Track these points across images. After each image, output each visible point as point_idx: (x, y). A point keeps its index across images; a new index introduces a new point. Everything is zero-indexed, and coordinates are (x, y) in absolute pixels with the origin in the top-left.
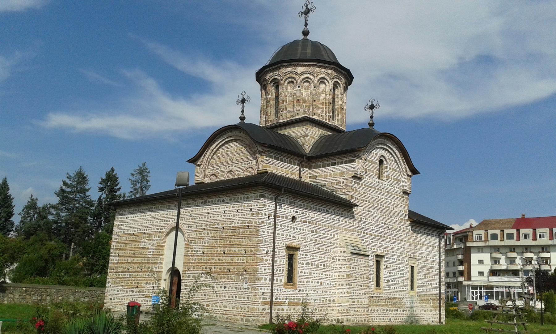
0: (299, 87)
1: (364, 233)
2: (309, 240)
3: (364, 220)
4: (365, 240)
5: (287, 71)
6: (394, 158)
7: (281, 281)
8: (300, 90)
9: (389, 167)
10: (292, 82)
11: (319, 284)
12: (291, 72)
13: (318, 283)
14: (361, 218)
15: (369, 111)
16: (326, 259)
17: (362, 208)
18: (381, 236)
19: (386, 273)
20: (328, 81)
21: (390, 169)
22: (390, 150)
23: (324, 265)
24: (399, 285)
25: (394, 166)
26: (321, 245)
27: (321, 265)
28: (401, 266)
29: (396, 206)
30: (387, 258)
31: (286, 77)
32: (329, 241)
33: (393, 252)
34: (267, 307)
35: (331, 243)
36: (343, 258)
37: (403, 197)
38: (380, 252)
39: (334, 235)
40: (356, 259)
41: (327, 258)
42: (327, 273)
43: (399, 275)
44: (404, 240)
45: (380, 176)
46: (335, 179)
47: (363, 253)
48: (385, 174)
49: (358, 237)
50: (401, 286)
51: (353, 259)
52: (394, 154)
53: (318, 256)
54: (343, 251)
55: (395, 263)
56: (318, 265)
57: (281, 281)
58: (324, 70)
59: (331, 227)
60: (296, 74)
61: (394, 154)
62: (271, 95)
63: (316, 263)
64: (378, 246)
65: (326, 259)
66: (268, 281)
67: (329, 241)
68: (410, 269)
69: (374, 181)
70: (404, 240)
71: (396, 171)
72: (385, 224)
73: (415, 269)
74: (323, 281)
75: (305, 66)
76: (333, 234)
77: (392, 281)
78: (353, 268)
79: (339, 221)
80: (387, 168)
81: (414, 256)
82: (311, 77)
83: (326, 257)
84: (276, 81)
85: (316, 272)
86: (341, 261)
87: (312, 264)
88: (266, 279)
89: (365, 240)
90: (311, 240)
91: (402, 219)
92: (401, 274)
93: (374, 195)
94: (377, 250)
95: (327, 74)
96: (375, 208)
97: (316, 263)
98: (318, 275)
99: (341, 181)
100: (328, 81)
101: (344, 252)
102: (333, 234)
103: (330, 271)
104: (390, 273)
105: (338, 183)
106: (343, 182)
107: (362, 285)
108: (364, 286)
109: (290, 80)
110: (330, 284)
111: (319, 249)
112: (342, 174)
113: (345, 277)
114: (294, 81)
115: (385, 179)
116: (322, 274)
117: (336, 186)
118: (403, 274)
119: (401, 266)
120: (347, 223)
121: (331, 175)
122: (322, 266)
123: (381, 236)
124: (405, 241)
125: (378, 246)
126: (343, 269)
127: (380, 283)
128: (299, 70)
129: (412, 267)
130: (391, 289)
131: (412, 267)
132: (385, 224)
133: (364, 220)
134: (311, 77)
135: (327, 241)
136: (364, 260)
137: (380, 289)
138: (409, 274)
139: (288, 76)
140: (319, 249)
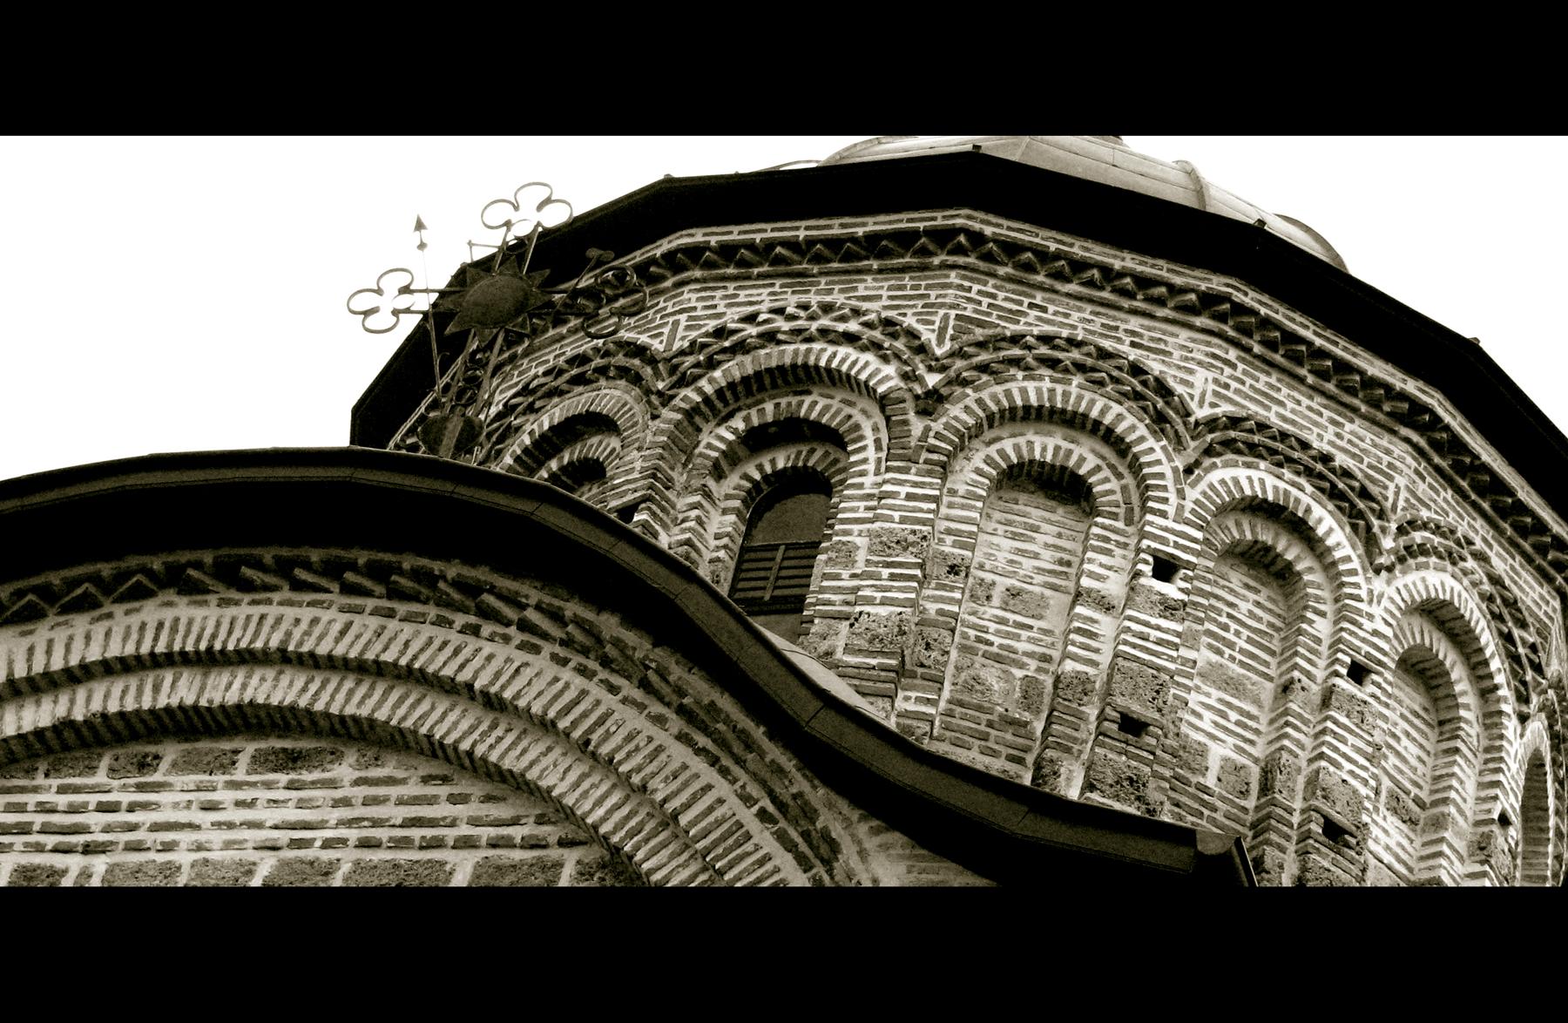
0: (1165, 569)
5: (1031, 324)
8: (1169, 608)
10: (1065, 488)
12: (1096, 365)
20: (1487, 692)
31: (993, 394)
60: (1159, 403)
75: (1286, 354)
82: (1326, 521)
84: (816, 406)
100: (1487, 692)
109: (1045, 445)
114: (1107, 486)
128: (1204, 374)
134: (1326, 521)
139: (1033, 389)
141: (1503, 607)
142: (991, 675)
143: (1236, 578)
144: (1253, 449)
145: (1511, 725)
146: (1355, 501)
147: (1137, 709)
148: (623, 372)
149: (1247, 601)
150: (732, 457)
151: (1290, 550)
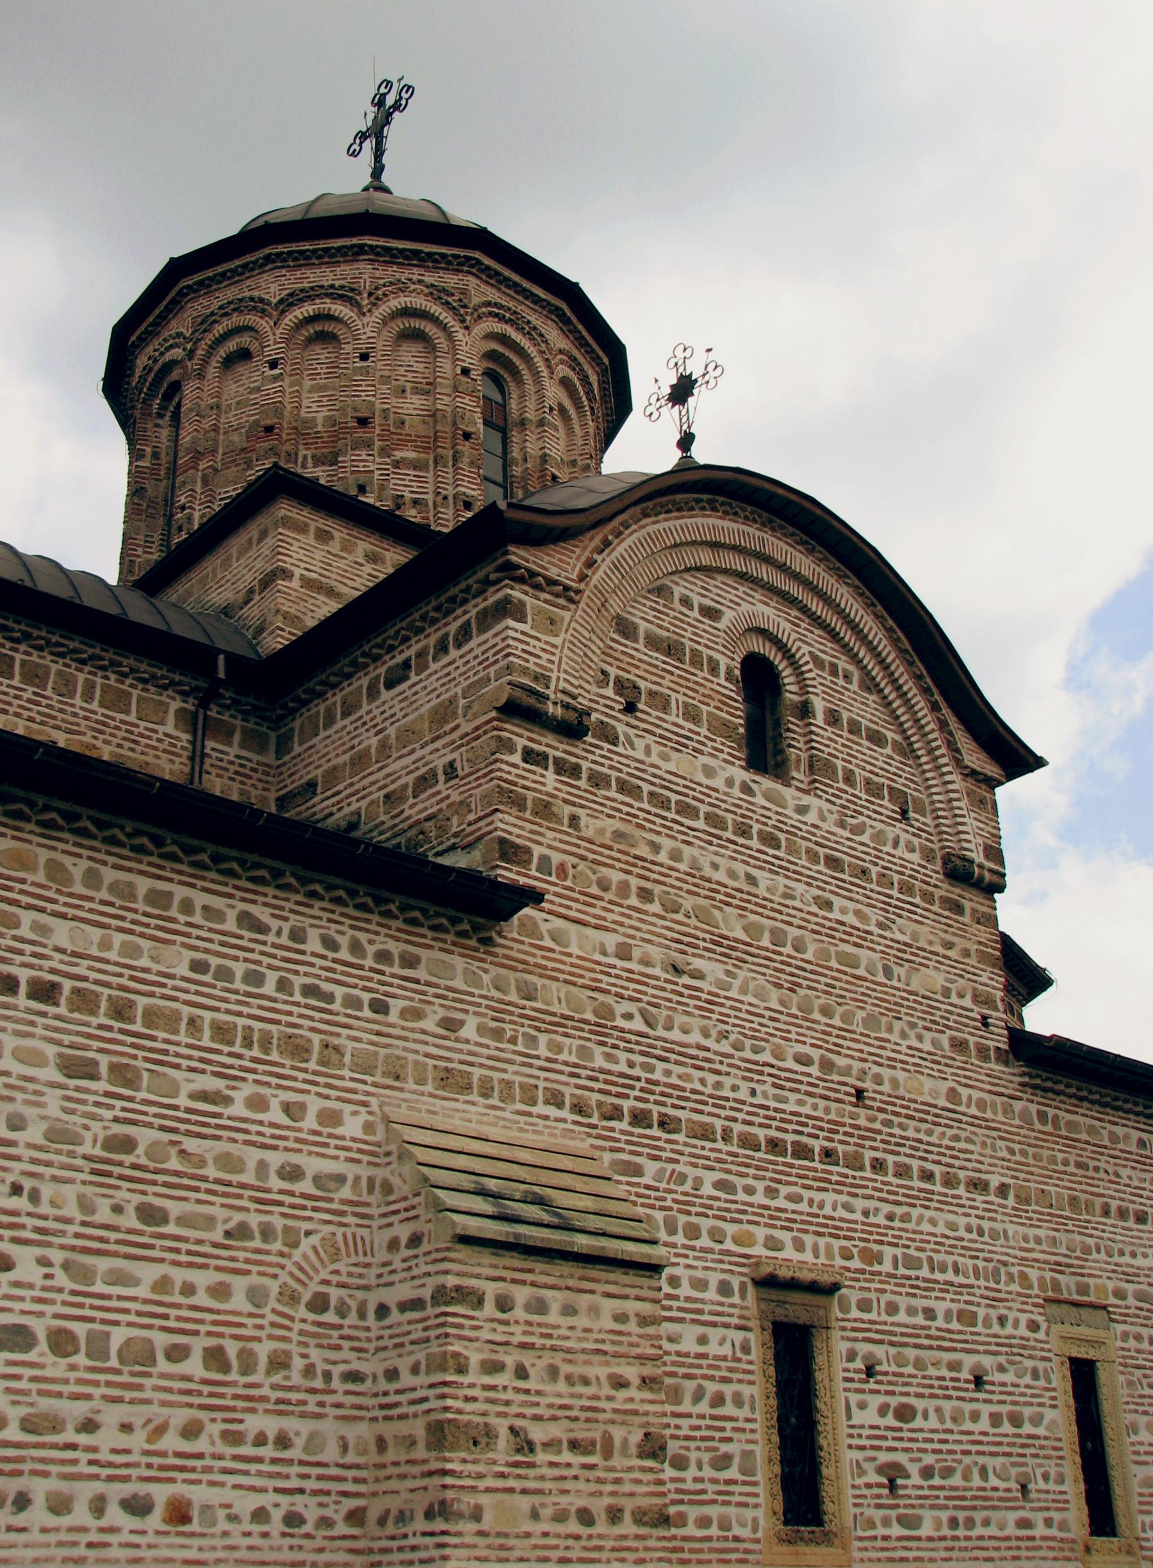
0: (273, 365)
1: (640, 1118)
2: (35, 1133)
3: (638, 1024)
4: (651, 1167)
6: (858, 662)
8: (276, 378)
9: (819, 705)
10: (244, 355)
11: (155, 1520)
13: (137, 1506)
14: (606, 1012)
15: (671, 414)
16: (239, 1302)
17: (611, 941)
18: (802, 1152)
19: (869, 1416)
20: (444, 327)
21: (833, 718)
22: (816, 606)
23: (215, 1358)
24: (983, 1499)
25: (864, 709)
26: (179, 1184)
27: (177, 1353)
28: (987, 1361)
30: (865, 1306)
31: (209, 338)
32: (275, 1159)
33: (912, 1263)
35: (293, 1173)
36: (405, 1292)
37: (958, 909)
38: (799, 1257)
39: (330, 1118)
40: (521, 1295)
41: (256, 1296)
42: (254, 1423)
43: (984, 1424)
44: (995, 1181)
45: (763, 750)
46: (401, 769)
47: (582, 1242)
48: (796, 751)
49: (583, 1145)
51: (491, 1290)
52: (848, 636)
53: (149, 1273)
54: (403, 1232)
55: (943, 1341)
56: (140, 1356)
59: (298, 1049)
60: (259, 306)
61: (848, 636)
62: (156, 455)
63: (118, 1336)
64: (775, 1216)
65: (239, 1302)
67: (275, 1159)
68: (1061, 1381)
69: (709, 772)
70: (995, 1181)
71: (876, 739)
72: (827, 1066)
73: (1114, 1387)
74: (199, 1495)
76: (314, 1105)
77: (927, 1473)
78: (494, 1367)
79: (380, 1007)
80: (805, 710)
81: (1083, 1289)
83: (239, 1284)
85: (111, 1416)
86: (395, 1316)
87: (62, 1342)
89: (651, 1167)
90: (58, 1135)
91: (959, 1045)
92: (995, 1419)
93: (721, 865)
94: (773, 1244)
97: (118, 1336)
98: (137, 1440)
99: (440, 763)
101: (415, 1240)
102: (314, 1105)
103: (282, 1407)
104: (905, 1413)
105: (425, 782)
106: (451, 771)
107: (598, 1506)
108: (614, 1515)
110: (293, 1519)
111: (150, 1215)
112: (444, 714)
113: (420, 1452)
115: (799, 775)
116: (191, 1431)
117: (414, 809)
118: (1016, 1420)
119: (987, 1361)
120: (469, 1031)
121: (384, 746)
122: (194, 1366)
123: (802, 1152)
124: (1003, 1190)
125: (775, 1216)
126: (407, 1379)
127: (827, 1490)
129: (1083, 1375)
130: (926, 1529)
131: (1083, 1375)
132: (827, 1066)
133: (638, 1024)
135: (253, 1156)
136: (609, 1305)
137: (828, 1539)
138: (1058, 1419)
140: (150, 1215)
141: (438, 293)
142: (235, 438)
143: (317, 349)
144: (301, 300)
145: (460, 335)
146: (346, 295)
147: (269, 422)
148: (490, 314)
149: (322, 353)
150: (163, 407)
151: (329, 327)
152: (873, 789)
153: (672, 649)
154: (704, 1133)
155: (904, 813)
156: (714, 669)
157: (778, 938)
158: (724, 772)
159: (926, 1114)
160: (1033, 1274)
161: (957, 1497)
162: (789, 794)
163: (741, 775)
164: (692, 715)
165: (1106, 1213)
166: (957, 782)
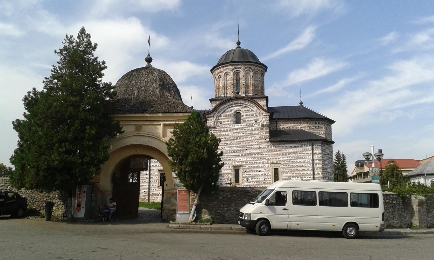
7: (155, 185)
9: (244, 115)
19: (245, 175)
21: (246, 115)
25: (251, 113)
29: (255, 136)
34: (147, 197)
37: (263, 129)
38: (237, 164)
50: (262, 181)
57: (155, 185)
58: (225, 68)
64: (235, 161)
66: (147, 186)
72: (242, 148)
80: (243, 116)
88: (146, 186)
93: (231, 134)
95: (228, 69)
96: (231, 141)
124: (266, 155)
125: (235, 161)
132: (242, 148)
152: (251, 121)
153: (226, 116)
154: (228, 156)
155: (256, 122)
156: (231, 116)
157: (237, 138)
158: (232, 125)
159: (255, 149)
160: (269, 162)
161: (255, 181)
162: (240, 125)
163: (233, 125)
164: (228, 121)
165: (283, 154)
166: (263, 116)
